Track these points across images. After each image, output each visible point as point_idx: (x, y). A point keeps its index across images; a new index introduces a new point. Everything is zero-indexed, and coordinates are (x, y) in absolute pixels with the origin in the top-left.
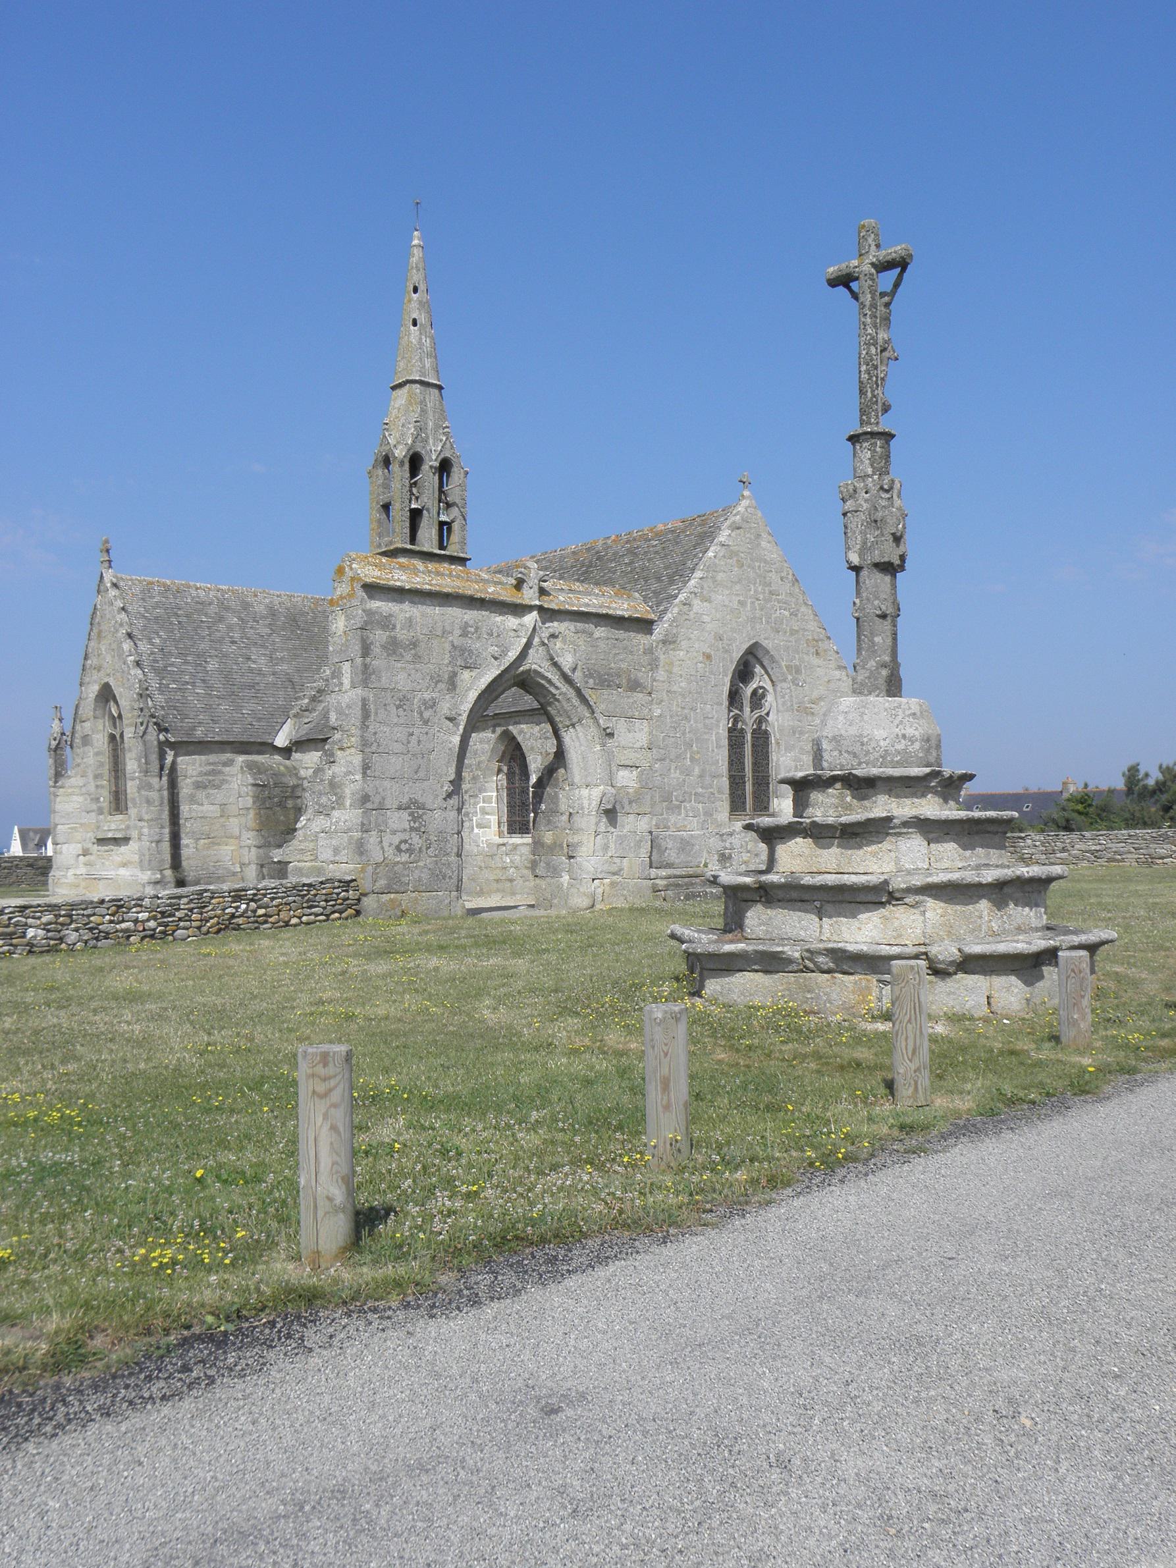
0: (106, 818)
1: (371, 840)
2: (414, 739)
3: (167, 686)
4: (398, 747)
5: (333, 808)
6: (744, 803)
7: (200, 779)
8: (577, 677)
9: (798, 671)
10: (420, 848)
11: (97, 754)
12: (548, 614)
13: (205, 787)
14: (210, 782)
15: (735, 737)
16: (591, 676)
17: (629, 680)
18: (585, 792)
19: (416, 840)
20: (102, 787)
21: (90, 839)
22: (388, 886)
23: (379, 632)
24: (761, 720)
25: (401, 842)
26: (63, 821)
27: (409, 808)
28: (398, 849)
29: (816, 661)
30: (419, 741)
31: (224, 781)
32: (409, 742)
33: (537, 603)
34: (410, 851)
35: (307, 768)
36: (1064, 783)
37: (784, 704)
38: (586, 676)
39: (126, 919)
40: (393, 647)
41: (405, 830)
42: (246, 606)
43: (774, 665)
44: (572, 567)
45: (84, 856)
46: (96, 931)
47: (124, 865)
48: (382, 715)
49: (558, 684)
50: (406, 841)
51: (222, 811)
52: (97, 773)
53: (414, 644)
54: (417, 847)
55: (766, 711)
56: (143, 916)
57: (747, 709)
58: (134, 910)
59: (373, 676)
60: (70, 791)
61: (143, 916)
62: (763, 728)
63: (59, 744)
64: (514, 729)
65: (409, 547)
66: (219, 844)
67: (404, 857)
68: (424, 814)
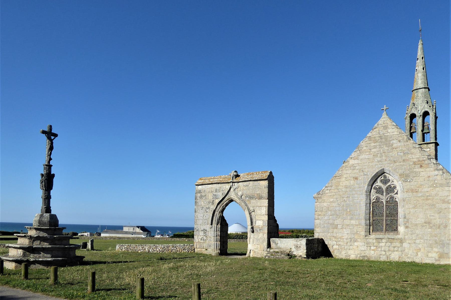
2: (204, 216)
4: (202, 218)
6: (382, 228)
12: (233, 182)
16: (247, 197)
22: (199, 247)
23: (199, 194)
30: (206, 216)
38: (246, 197)
40: (201, 197)
53: (205, 196)
55: (395, 193)
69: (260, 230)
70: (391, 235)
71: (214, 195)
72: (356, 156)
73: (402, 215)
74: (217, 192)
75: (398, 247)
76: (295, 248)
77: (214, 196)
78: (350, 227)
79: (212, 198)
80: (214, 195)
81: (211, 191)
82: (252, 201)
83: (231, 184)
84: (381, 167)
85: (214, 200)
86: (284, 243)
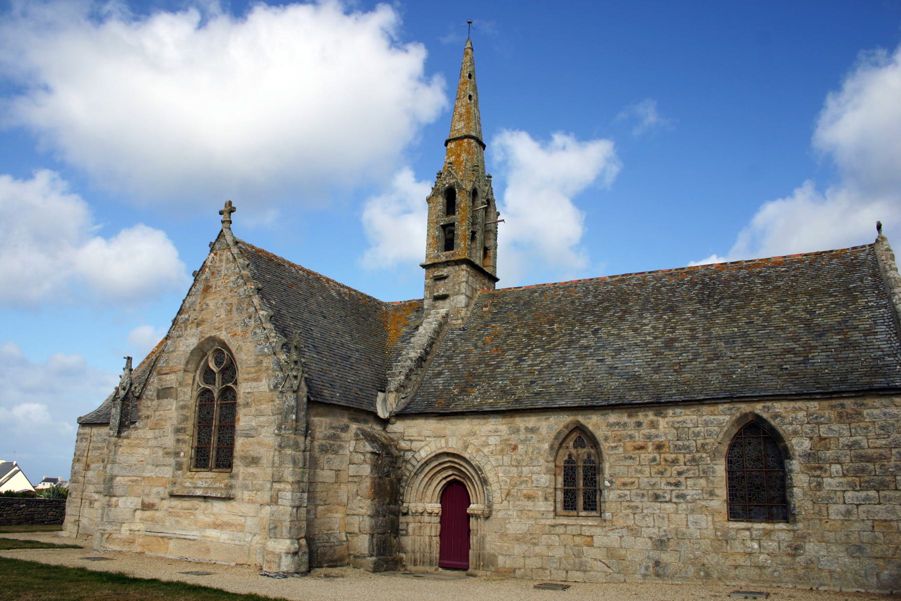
0: (183, 474)
7: (324, 442)
11: (183, 407)
13: (327, 451)
20: (184, 442)
21: (158, 493)
26: (124, 472)
31: (341, 447)
35: (411, 441)
45: (143, 510)
47: (216, 526)
51: (337, 476)
52: (180, 426)
63: (127, 393)
64: (594, 422)
66: (331, 511)
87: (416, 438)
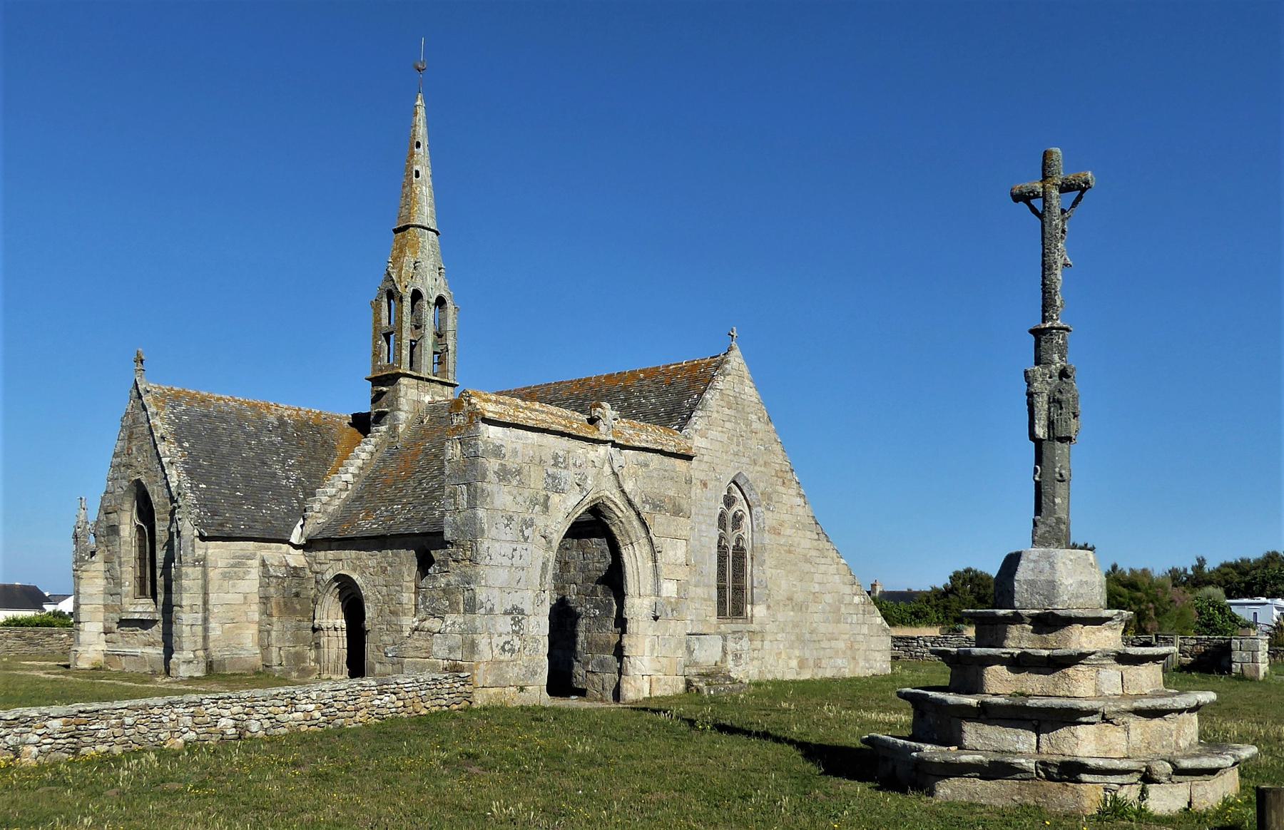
1: (483, 641)
2: (517, 554)
3: (197, 486)
5: (448, 613)
8: (637, 501)
9: (770, 499)
10: (519, 649)
13: (231, 578)
14: (235, 573)
15: (722, 550)
17: (674, 505)
18: (637, 601)
19: (517, 643)
22: (496, 681)
23: (492, 460)
24: (739, 539)
25: (505, 643)
27: (512, 613)
28: (503, 648)
29: (781, 489)
30: (521, 556)
32: (513, 557)
33: (611, 438)
34: (512, 651)
36: (872, 585)
37: (758, 525)
39: (298, 709)
41: (509, 633)
42: (261, 417)
43: (752, 493)
44: (568, 399)
46: (274, 720)
48: (494, 532)
49: (625, 511)
50: (509, 642)
51: (245, 598)
53: (519, 472)
54: (516, 648)
56: (311, 707)
57: (729, 529)
58: (304, 702)
59: (488, 499)
60: (94, 574)
61: (311, 707)
62: (741, 545)
65: (408, 372)
66: (241, 628)
67: (508, 655)
68: (523, 618)
69: (672, 610)
70: (739, 625)
71: (549, 475)
72: (703, 429)
73: (762, 581)
74: (560, 467)
75: (759, 650)
76: (733, 660)
77: (550, 481)
78: (696, 605)
79: (541, 485)
80: (549, 475)
81: (538, 459)
82: (660, 518)
83: (602, 450)
84: (738, 468)
85: (549, 494)
86: (705, 647)
87: (323, 561)
